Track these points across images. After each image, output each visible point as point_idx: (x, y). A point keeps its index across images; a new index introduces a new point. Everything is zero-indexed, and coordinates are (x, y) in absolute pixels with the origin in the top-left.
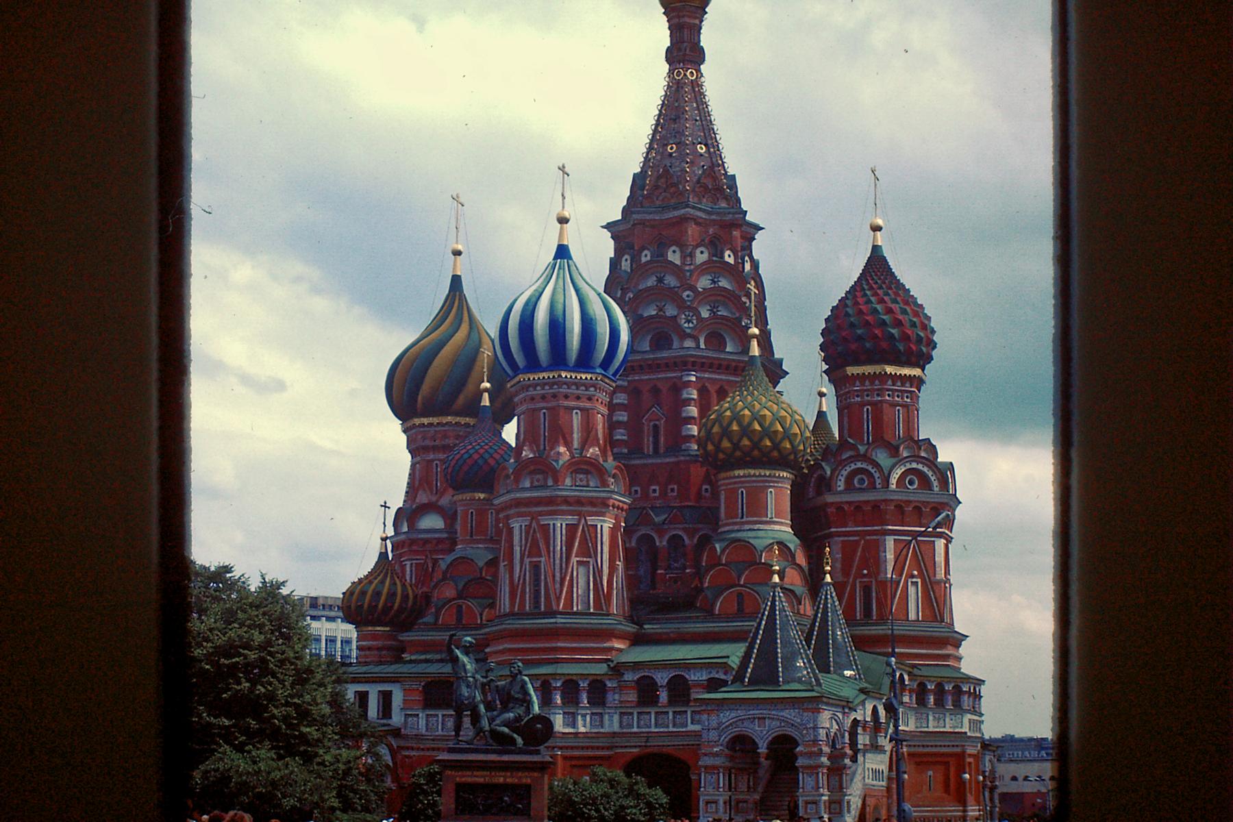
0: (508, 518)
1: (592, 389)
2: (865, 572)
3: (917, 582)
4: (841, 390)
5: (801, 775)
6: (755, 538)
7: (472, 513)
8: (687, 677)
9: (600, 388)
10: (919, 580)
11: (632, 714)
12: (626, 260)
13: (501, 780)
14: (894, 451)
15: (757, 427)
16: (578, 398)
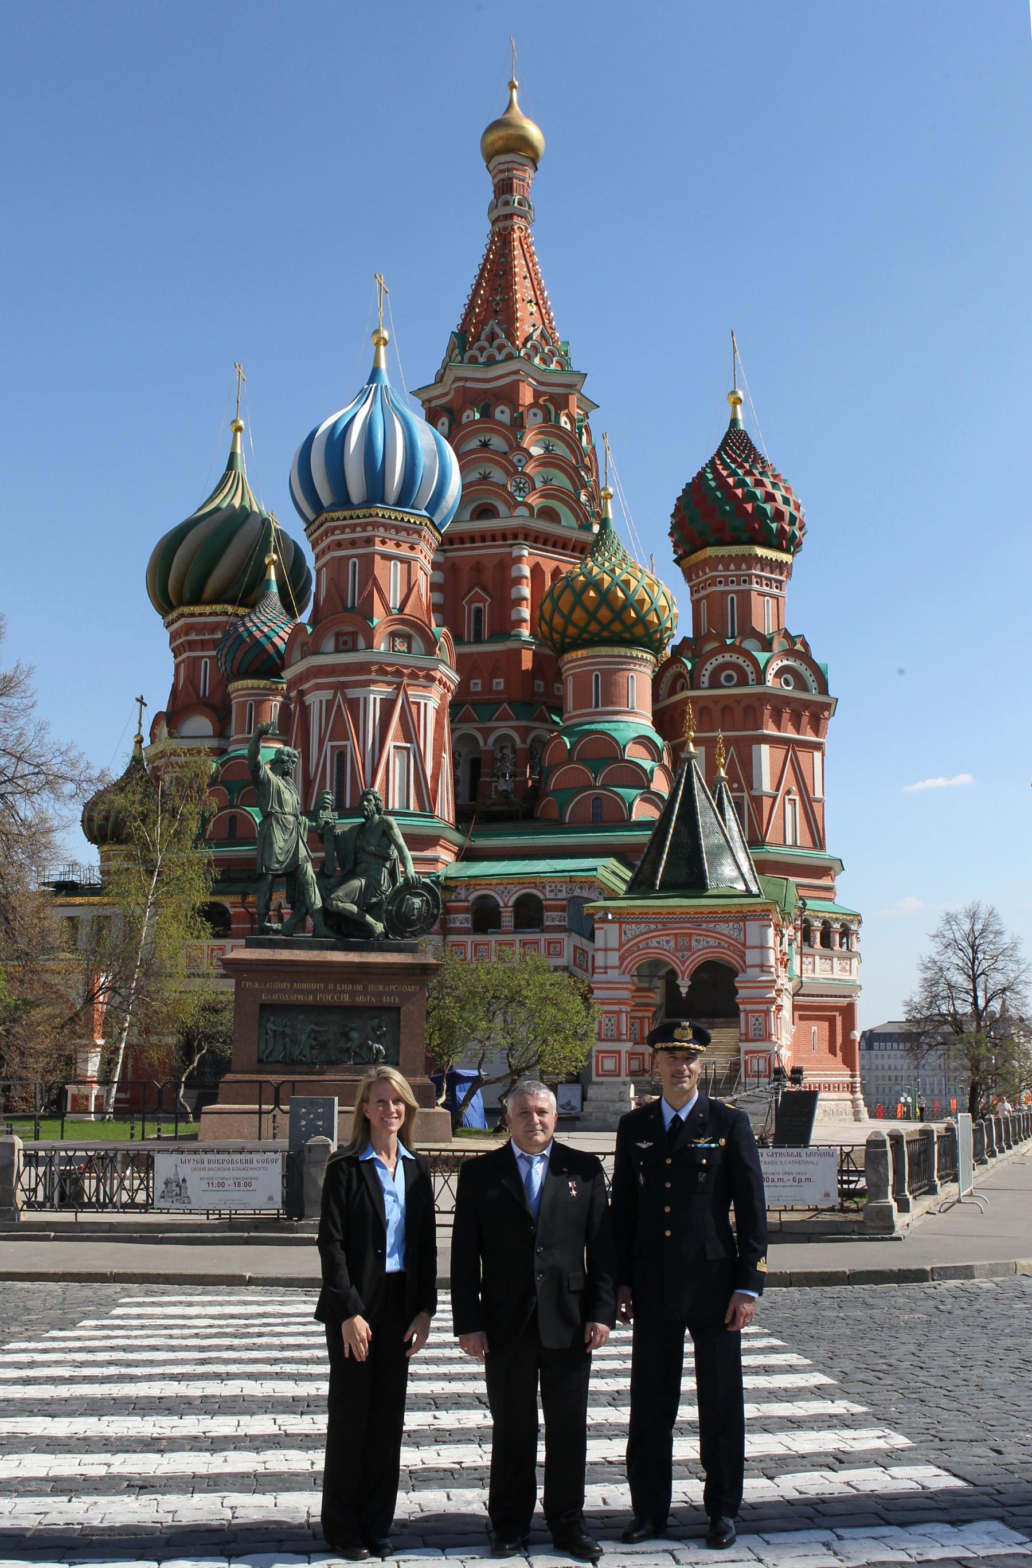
0: (302, 694)
1: (416, 536)
2: (735, 786)
3: (794, 800)
4: (698, 577)
5: (742, 1015)
6: (615, 730)
7: (251, 705)
8: (542, 897)
9: (425, 536)
10: (797, 798)
11: (463, 945)
12: (443, 424)
13: (346, 998)
14: (766, 644)
15: (620, 594)
16: (398, 545)
